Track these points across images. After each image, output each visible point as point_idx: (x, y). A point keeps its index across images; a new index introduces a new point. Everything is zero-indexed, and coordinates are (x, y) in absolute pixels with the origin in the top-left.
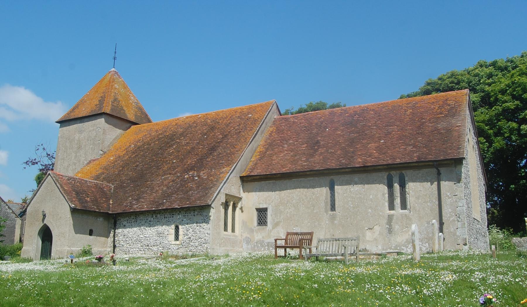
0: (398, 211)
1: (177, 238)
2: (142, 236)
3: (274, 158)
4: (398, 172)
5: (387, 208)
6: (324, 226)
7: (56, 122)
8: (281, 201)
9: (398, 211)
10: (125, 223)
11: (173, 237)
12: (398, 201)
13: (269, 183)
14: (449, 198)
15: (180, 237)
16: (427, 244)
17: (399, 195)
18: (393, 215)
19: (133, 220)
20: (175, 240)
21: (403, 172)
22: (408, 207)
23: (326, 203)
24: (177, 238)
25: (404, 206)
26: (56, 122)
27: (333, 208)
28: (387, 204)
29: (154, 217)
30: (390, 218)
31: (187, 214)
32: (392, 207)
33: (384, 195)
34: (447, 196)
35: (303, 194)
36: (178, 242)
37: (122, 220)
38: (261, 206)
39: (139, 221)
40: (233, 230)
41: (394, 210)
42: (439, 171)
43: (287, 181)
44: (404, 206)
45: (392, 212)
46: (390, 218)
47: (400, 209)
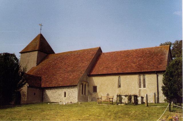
0: (142, 88)
1: (65, 96)
3: (99, 68)
7: (20, 53)
9: (142, 88)
11: (63, 96)
12: (142, 85)
15: (66, 96)
22: (146, 87)
24: (65, 96)
26: (20, 53)
27: (119, 86)
30: (140, 90)
32: (140, 87)
40: (85, 94)
44: (144, 86)
45: (140, 89)
46: (140, 90)
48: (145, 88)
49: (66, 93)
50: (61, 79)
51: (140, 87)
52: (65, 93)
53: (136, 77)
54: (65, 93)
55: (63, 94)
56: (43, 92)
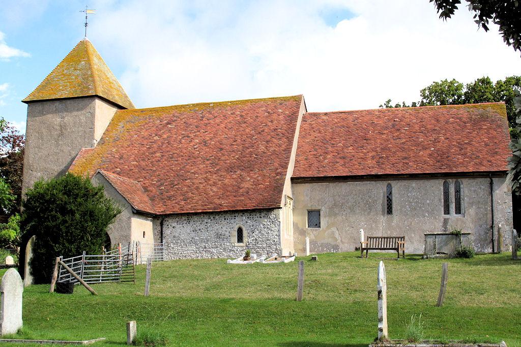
0: (453, 215)
2: (197, 238)
4: (454, 180)
5: (443, 212)
6: (381, 228)
8: (335, 203)
10: (174, 224)
13: (322, 185)
14: (500, 205)
15: (245, 239)
16: (479, 245)
17: (454, 200)
18: (448, 219)
19: (185, 222)
20: (238, 242)
21: (459, 180)
23: (383, 205)
25: (458, 210)
28: (443, 209)
29: (212, 218)
31: (251, 216)
32: (447, 211)
33: (440, 200)
34: (498, 203)
35: (359, 197)
36: (241, 244)
37: (170, 221)
38: (314, 208)
39: (192, 223)
41: (449, 214)
42: (492, 181)
43: (342, 183)
44: (458, 210)
45: (447, 216)
47: (454, 213)
48: (459, 216)
49: (244, 230)
50: (215, 189)
51: (447, 211)
52: (240, 231)
53: (437, 186)
54: (240, 231)
55: (236, 234)
56: (162, 224)
